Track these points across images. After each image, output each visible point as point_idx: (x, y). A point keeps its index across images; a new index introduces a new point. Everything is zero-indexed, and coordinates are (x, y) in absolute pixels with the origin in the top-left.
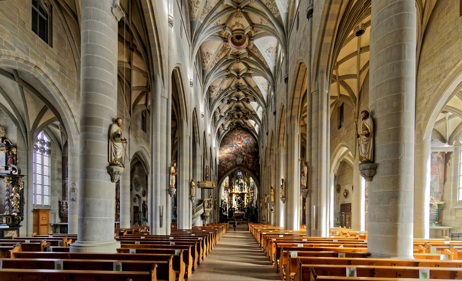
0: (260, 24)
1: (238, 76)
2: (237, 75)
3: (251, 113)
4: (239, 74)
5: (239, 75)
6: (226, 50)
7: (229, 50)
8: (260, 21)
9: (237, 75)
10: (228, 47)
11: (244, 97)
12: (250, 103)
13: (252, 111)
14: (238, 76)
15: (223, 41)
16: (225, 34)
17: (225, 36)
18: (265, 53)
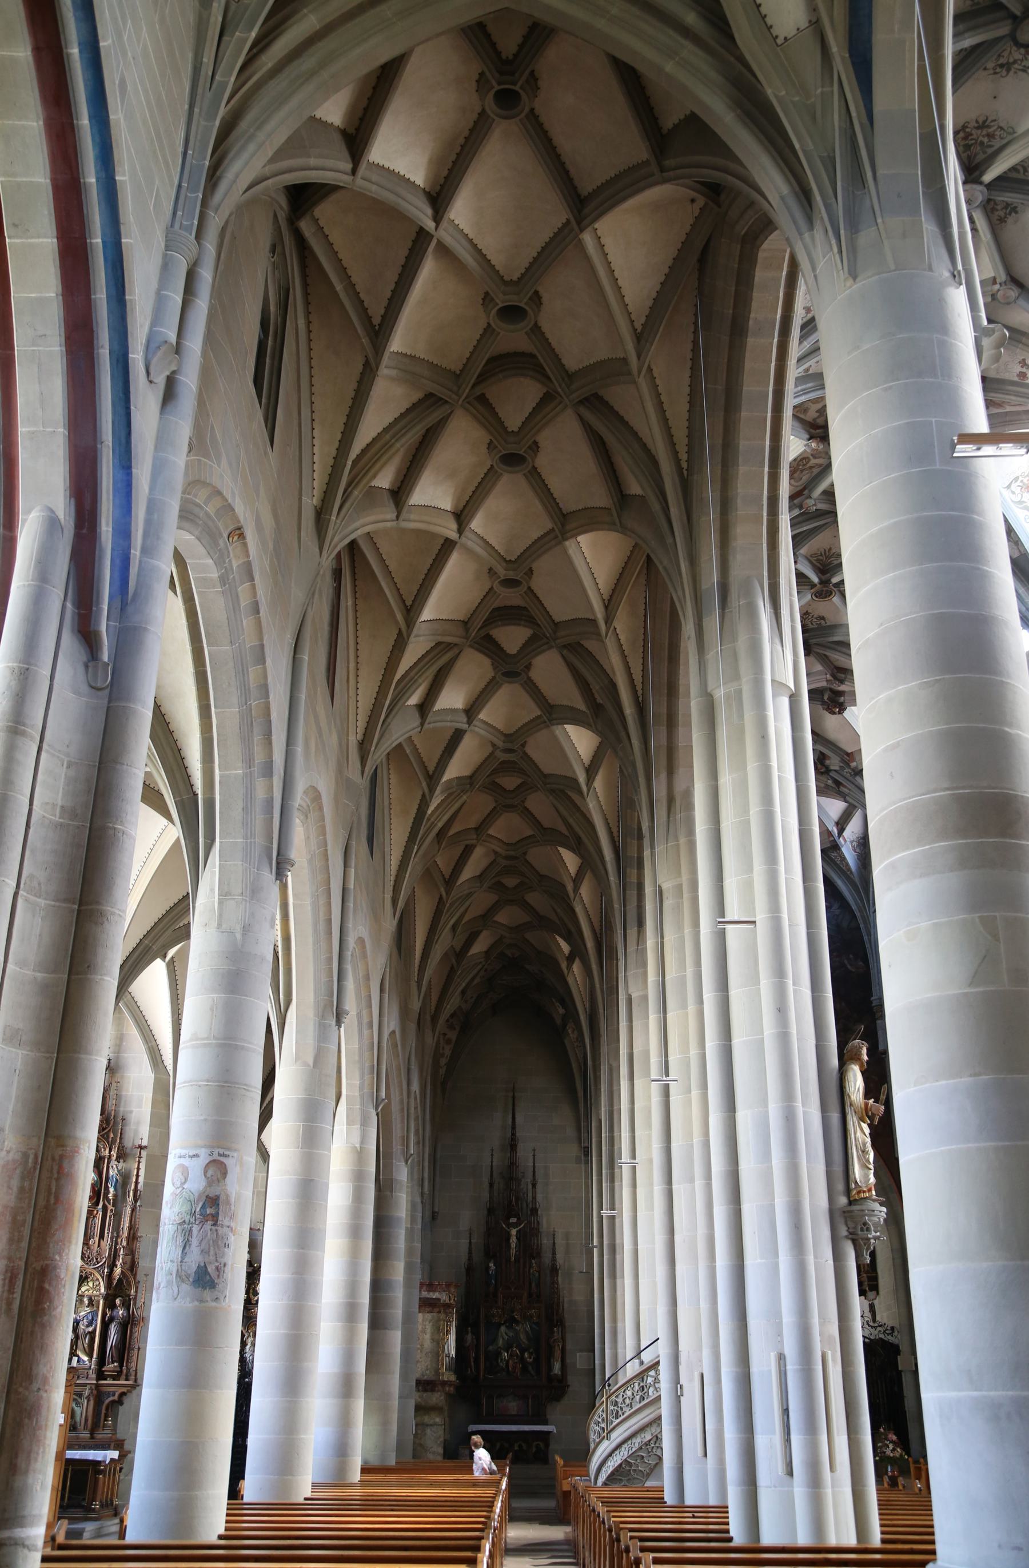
0: (1016, 379)
1: (825, 582)
2: (815, 579)
3: (843, 761)
4: (824, 578)
5: (828, 581)
6: (802, 471)
7: (816, 471)
8: (1018, 369)
9: (815, 579)
10: (813, 461)
11: (824, 684)
12: (847, 714)
13: (848, 754)
14: (825, 582)
15: (808, 436)
16: (817, 412)
17: (819, 417)
18: (1006, 493)
